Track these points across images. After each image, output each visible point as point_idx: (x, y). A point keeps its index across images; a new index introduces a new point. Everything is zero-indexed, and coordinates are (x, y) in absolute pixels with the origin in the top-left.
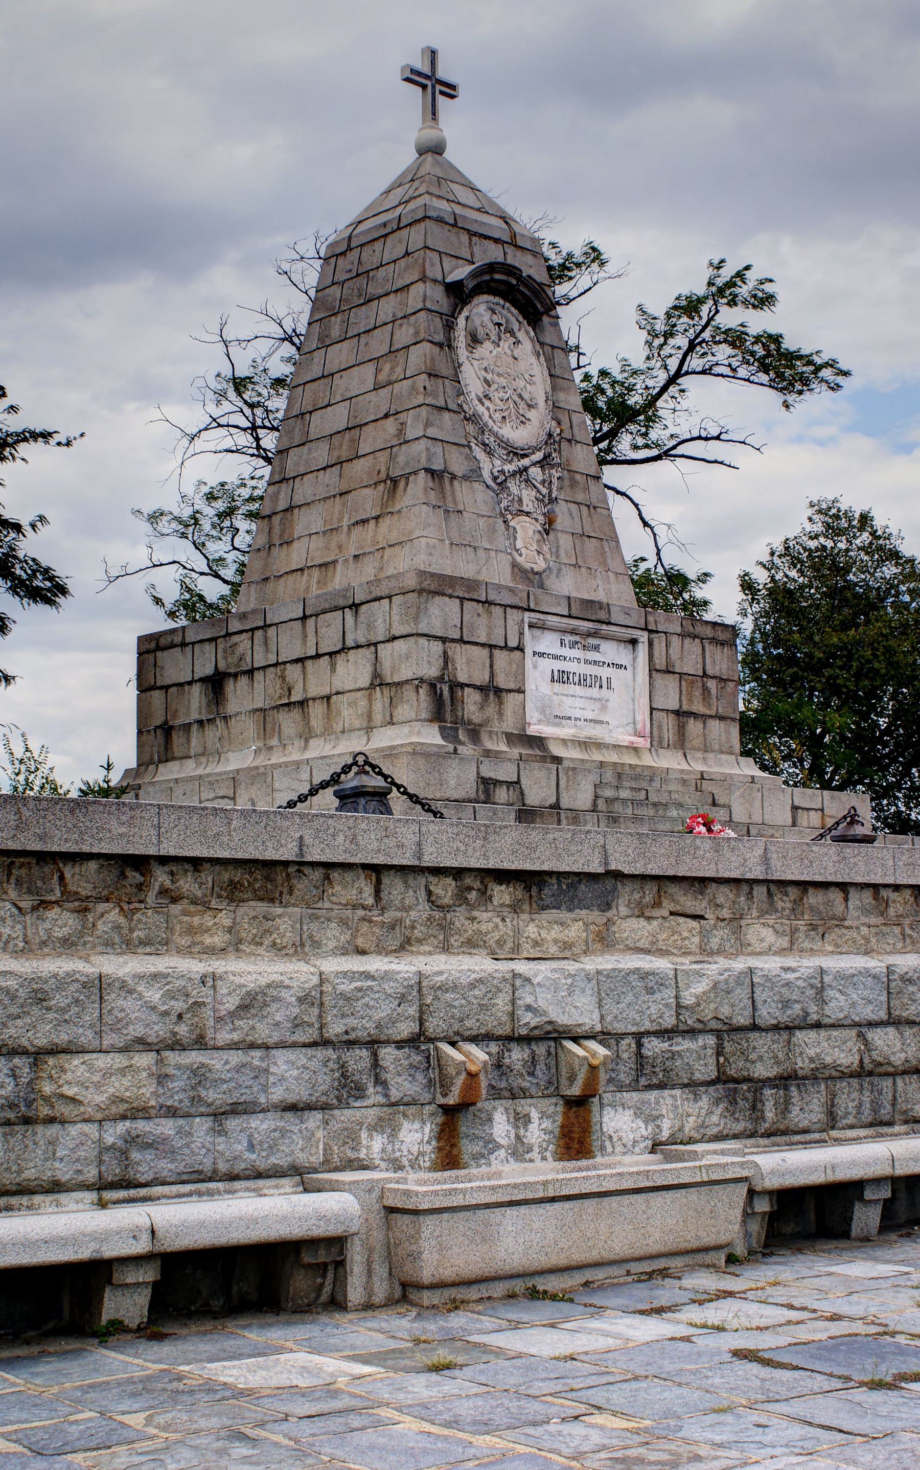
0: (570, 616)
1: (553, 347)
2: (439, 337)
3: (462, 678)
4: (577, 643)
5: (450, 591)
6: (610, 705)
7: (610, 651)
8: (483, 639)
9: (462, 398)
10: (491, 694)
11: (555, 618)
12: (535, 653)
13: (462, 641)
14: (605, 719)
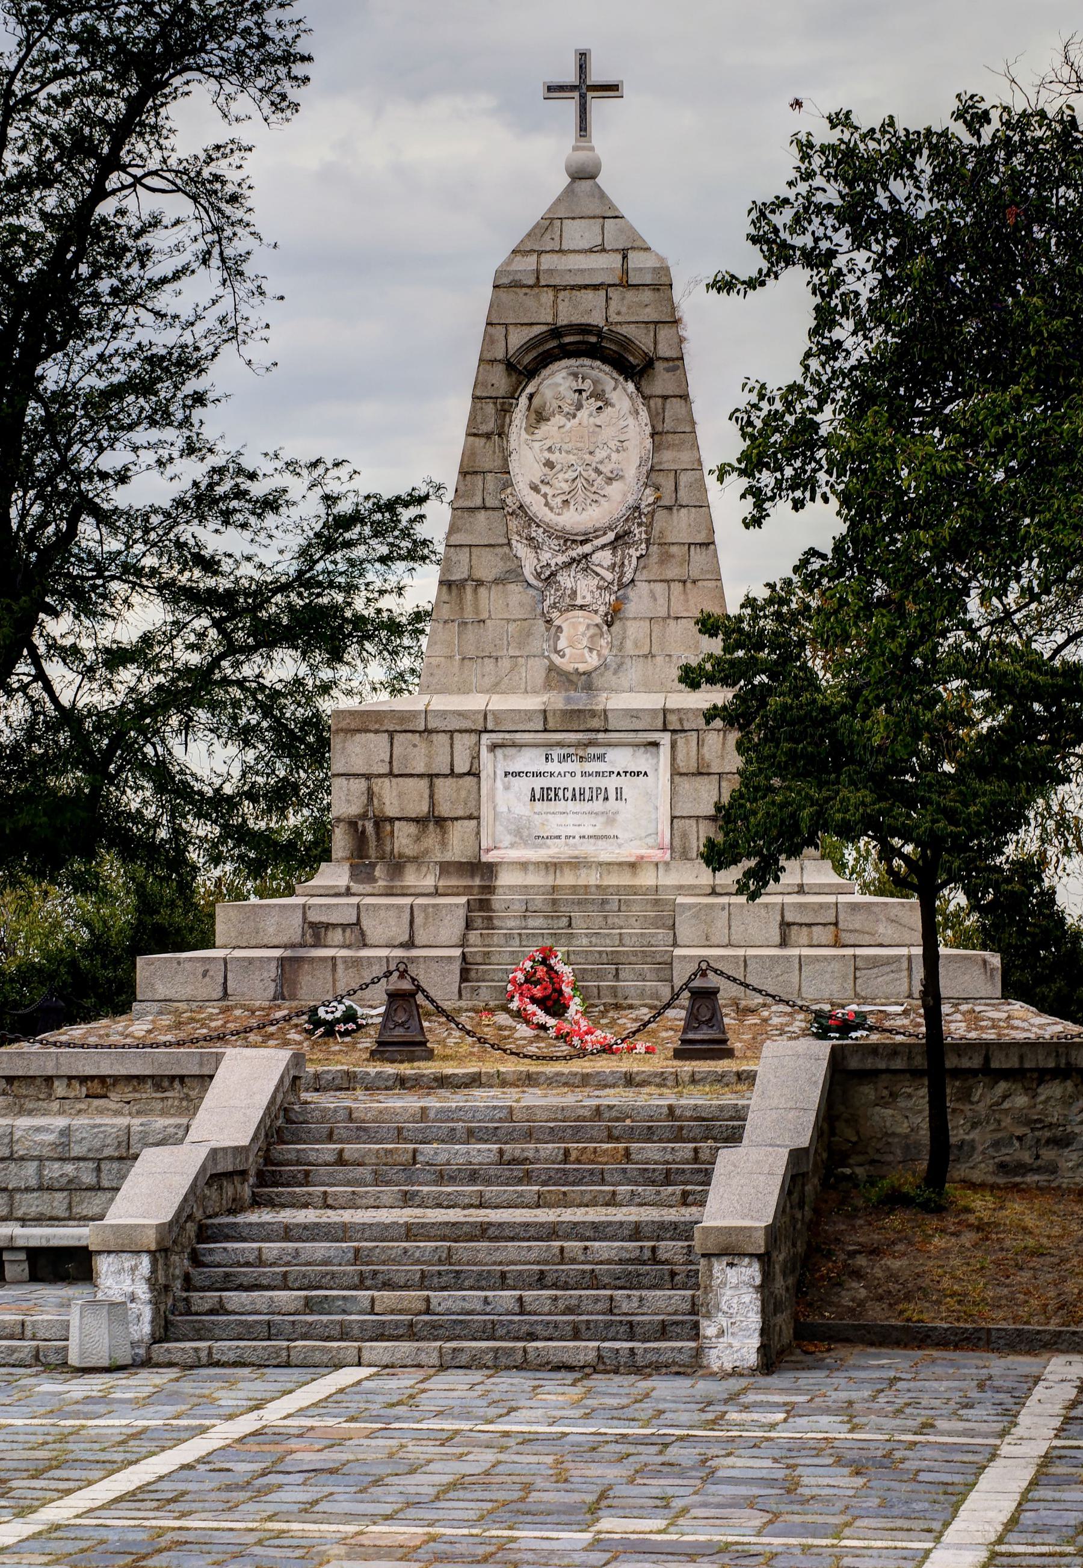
0: (545, 731)
1: (665, 398)
2: (490, 426)
3: (391, 811)
4: (569, 755)
5: (377, 726)
6: (619, 818)
7: (620, 758)
8: (420, 769)
9: (509, 491)
10: (431, 826)
11: (526, 735)
12: (506, 774)
13: (391, 774)
14: (615, 832)
